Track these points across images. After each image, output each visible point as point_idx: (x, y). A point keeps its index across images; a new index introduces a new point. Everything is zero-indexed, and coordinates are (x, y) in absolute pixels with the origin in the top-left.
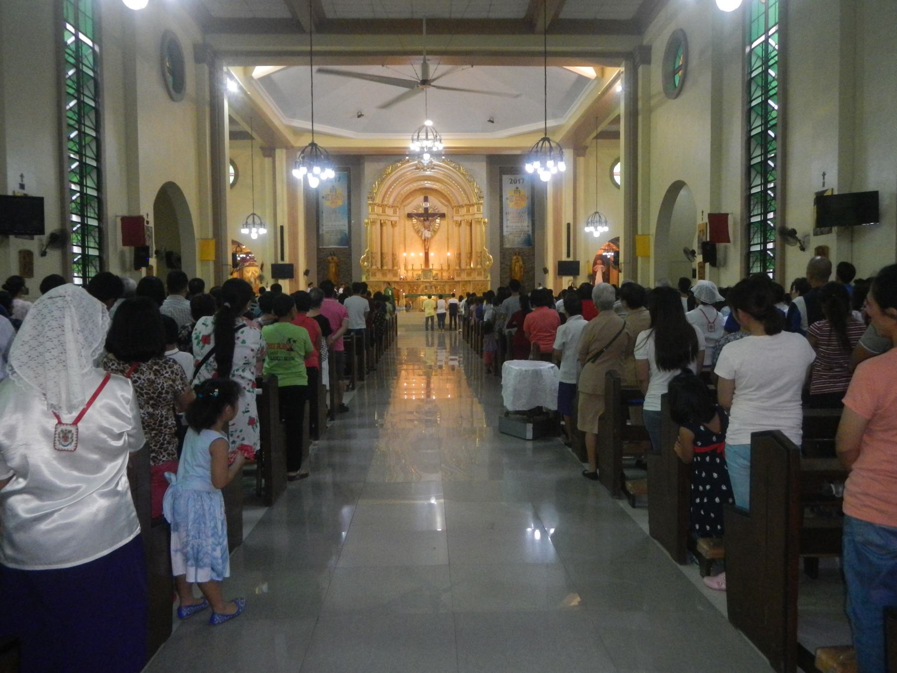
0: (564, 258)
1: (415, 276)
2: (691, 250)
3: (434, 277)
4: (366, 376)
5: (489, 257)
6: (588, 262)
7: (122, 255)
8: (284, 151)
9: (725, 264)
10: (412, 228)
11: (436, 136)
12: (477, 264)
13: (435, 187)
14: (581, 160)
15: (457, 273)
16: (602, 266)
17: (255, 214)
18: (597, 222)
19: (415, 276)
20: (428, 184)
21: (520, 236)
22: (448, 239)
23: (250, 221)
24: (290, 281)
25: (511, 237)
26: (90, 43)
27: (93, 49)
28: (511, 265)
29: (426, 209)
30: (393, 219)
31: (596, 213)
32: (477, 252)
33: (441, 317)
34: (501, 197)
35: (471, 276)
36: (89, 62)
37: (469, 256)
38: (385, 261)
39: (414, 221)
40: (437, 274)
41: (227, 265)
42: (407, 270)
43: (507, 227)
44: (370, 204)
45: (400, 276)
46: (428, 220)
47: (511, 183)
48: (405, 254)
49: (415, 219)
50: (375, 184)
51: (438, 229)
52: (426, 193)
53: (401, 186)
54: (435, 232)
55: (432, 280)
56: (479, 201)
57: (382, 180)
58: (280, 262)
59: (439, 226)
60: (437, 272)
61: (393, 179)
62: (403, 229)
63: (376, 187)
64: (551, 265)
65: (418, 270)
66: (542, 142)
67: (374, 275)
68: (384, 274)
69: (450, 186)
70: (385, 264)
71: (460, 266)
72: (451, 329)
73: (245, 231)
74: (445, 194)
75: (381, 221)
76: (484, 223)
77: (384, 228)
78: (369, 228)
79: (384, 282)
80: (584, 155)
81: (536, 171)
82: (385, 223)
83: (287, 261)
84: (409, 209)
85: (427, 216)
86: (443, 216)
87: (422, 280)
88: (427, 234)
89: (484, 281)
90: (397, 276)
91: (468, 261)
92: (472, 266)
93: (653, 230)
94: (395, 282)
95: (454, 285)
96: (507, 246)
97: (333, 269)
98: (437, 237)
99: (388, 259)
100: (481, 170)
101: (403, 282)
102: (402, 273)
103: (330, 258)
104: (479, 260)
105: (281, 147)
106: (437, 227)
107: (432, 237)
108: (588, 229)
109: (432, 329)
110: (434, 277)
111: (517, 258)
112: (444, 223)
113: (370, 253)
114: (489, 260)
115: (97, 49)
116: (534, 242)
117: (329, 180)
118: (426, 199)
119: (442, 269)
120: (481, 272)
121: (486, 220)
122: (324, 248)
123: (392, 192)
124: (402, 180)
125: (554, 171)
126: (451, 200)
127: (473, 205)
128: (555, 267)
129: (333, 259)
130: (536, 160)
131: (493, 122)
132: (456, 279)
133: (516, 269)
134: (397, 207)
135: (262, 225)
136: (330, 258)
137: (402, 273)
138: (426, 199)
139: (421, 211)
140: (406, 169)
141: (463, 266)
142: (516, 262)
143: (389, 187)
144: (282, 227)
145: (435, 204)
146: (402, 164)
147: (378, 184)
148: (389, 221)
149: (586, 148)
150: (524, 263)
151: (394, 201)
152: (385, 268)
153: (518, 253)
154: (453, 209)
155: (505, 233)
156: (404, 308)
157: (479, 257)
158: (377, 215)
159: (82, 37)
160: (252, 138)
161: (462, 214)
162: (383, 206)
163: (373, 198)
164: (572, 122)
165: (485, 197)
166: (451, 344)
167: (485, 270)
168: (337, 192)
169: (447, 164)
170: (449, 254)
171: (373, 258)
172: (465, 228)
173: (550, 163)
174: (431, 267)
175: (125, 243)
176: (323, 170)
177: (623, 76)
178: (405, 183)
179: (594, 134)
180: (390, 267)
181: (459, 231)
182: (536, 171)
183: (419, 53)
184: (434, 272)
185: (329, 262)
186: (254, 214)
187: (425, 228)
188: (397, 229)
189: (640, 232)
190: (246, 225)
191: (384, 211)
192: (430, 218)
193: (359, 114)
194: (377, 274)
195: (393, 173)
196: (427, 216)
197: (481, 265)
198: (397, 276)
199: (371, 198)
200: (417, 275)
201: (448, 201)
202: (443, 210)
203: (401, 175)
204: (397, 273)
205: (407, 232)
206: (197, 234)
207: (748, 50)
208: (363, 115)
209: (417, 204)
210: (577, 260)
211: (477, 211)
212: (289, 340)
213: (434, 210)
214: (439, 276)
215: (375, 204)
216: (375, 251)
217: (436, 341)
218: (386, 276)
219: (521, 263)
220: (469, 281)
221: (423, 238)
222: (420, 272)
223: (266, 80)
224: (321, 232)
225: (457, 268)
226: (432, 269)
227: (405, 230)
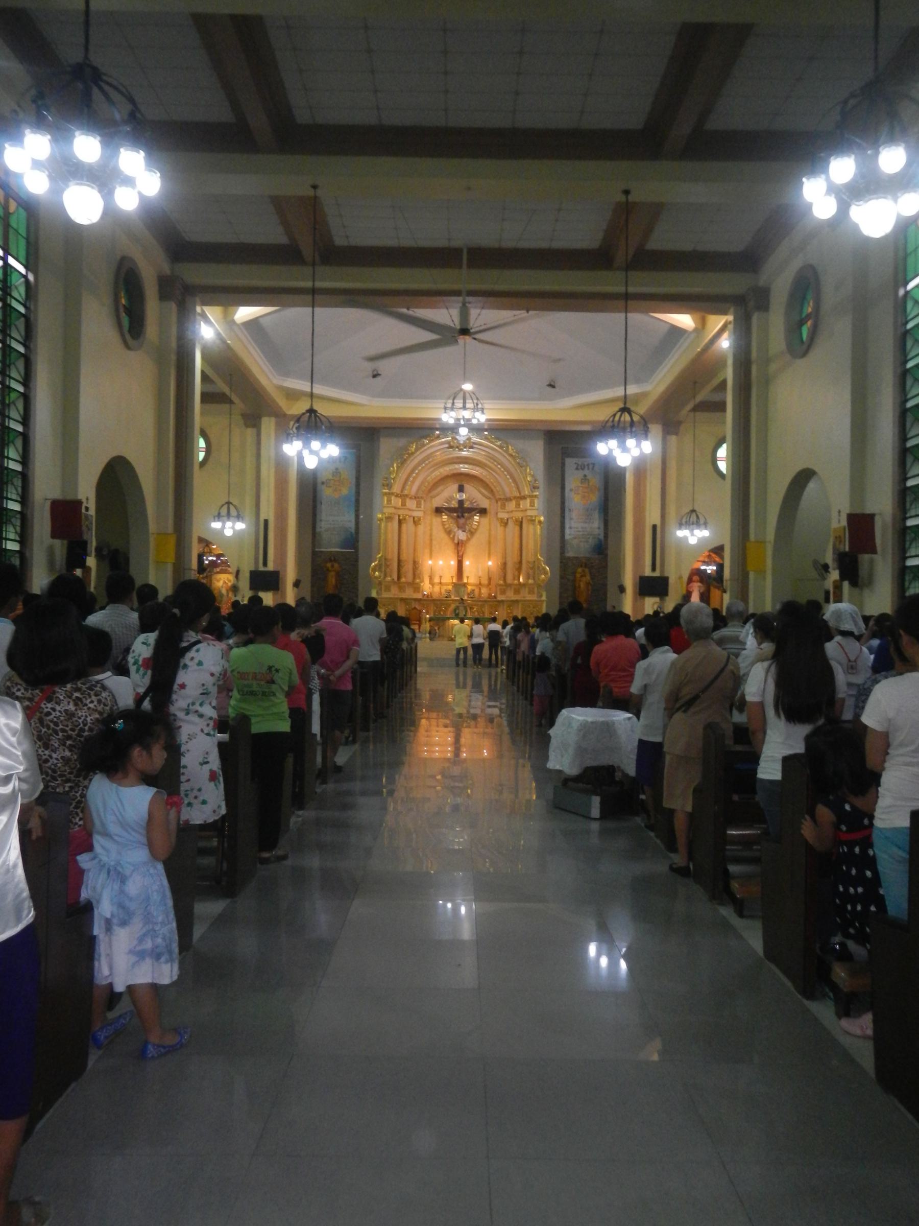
0: (648, 572)
1: (443, 591)
2: (822, 563)
4: (372, 725)
5: (544, 569)
6: (680, 578)
7: (51, 551)
8: (273, 420)
9: (870, 582)
10: (441, 528)
11: (477, 404)
13: (474, 472)
14: (673, 439)
15: (500, 589)
16: (699, 584)
17: (231, 503)
18: (693, 524)
19: (443, 591)
20: (464, 468)
21: (587, 542)
22: (489, 543)
23: (224, 511)
24: (273, 595)
25: (575, 542)
26: (22, 270)
27: (25, 277)
28: (574, 581)
29: (461, 502)
30: (416, 514)
31: (693, 511)
32: (529, 562)
33: (478, 648)
34: (563, 488)
36: (20, 295)
37: (517, 566)
38: (403, 570)
39: (445, 517)
40: (473, 590)
41: (191, 570)
43: (570, 528)
44: (386, 493)
45: (423, 591)
46: (463, 516)
47: (577, 469)
48: (430, 562)
49: (446, 515)
50: (393, 468)
51: (476, 530)
52: (462, 480)
53: (429, 469)
54: (472, 533)
56: (533, 492)
57: (403, 462)
58: (261, 568)
59: (478, 526)
60: (473, 588)
61: (416, 461)
62: (429, 528)
63: (394, 471)
64: (629, 582)
65: (447, 584)
66: (619, 414)
67: (388, 589)
68: (401, 588)
69: (496, 473)
71: (505, 580)
72: (490, 665)
73: (216, 525)
74: (488, 482)
75: (399, 516)
76: (540, 522)
77: (404, 527)
78: (383, 525)
79: (402, 600)
80: (676, 434)
81: (611, 451)
82: (405, 519)
83: (271, 567)
84: (438, 502)
85: (461, 512)
86: (483, 512)
88: (462, 535)
89: (536, 601)
90: (419, 592)
91: (516, 573)
92: (521, 580)
93: (770, 535)
94: (416, 600)
96: (570, 554)
97: (332, 580)
98: (474, 541)
99: (408, 568)
100: (536, 450)
101: (429, 601)
102: (426, 588)
103: (329, 565)
104: (531, 572)
105: (269, 415)
106: (475, 527)
107: (468, 539)
108: (681, 533)
109: (465, 664)
110: (469, 594)
111: (583, 571)
112: (485, 521)
113: (383, 560)
114: (545, 573)
115: (31, 277)
116: (606, 548)
117: (331, 460)
118: (461, 489)
119: (480, 584)
120: (533, 588)
121: (542, 519)
122: (321, 552)
123: (415, 478)
124: (430, 462)
125: (636, 452)
126: (494, 490)
127: (524, 498)
128: (634, 586)
129: (333, 566)
130: (612, 438)
131: (553, 387)
132: (500, 598)
134: (422, 498)
135: (239, 517)
136: (329, 565)
137: (426, 588)
138: (461, 489)
139: (454, 504)
140: (436, 447)
141: (509, 579)
142: (582, 576)
143: (413, 471)
144: (266, 522)
145: (473, 495)
146: (431, 441)
147: (398, 467)
148: (410, 516)
149: (679, 423)
150: (592, 579)
151: (418, 490)
152: (403, 580)
153: (585, 564)
154: (497, 502)
155: (567, 537)
156: (428, 635)
157: (532, 568)
158: (395, 508)
159: (11, 261)
160: (231, 402)
161: (511, 510)
162: (403, 496)
163: (390, 488)
164: (662, 388)
165: (542, 489)
166: (490, 686)
167: (539, 586)
168: (342, 478)
169: (492, 443)
170: (490, 563)
171: (387, 566)
172: (512, 528)
173: (631, 442)
174: (465, 581)
175: (55, 535)
176: (324, 446)
177: (731, 327)
178: (433, 466)
179: (690, 406)
180: (410, 579)
181: (505, 531)
182: (611, 451)
183: (457, 293)
184: (470, 588)
185: (328, 570)
186: (229, 503)
187: (459, 527)
188: (421, 528)
189: (752, 537)
190: (218, 517)
191: (404, 504)
192: (466, 515)
193: (375, 373)
195: (418, 453)
196: (461, 512)
197: (534, 579)
199: (388, 485)
200: (446, 591)
201: (492, 491)
202: (485, 503)
203: (429, 455)
205: (434, 532)
206: (152, 527)
207: (901, 292)
208: (379, 375)
209: (449, 494)
210: (666, 575)
211: (531, 506)
212: (270, 668)
213: (471, 503)
215: (393, 494)
216: (389, 557)
217: (469, 682)
218: (404, 591)
219: (588, 578)
220: (517, 601)
221: (456, 541)
222: (450, 587)
223: (252, 325)
224: (318, 530)
225: (501, 582)
226: (467, 583)
227: (431, 529)
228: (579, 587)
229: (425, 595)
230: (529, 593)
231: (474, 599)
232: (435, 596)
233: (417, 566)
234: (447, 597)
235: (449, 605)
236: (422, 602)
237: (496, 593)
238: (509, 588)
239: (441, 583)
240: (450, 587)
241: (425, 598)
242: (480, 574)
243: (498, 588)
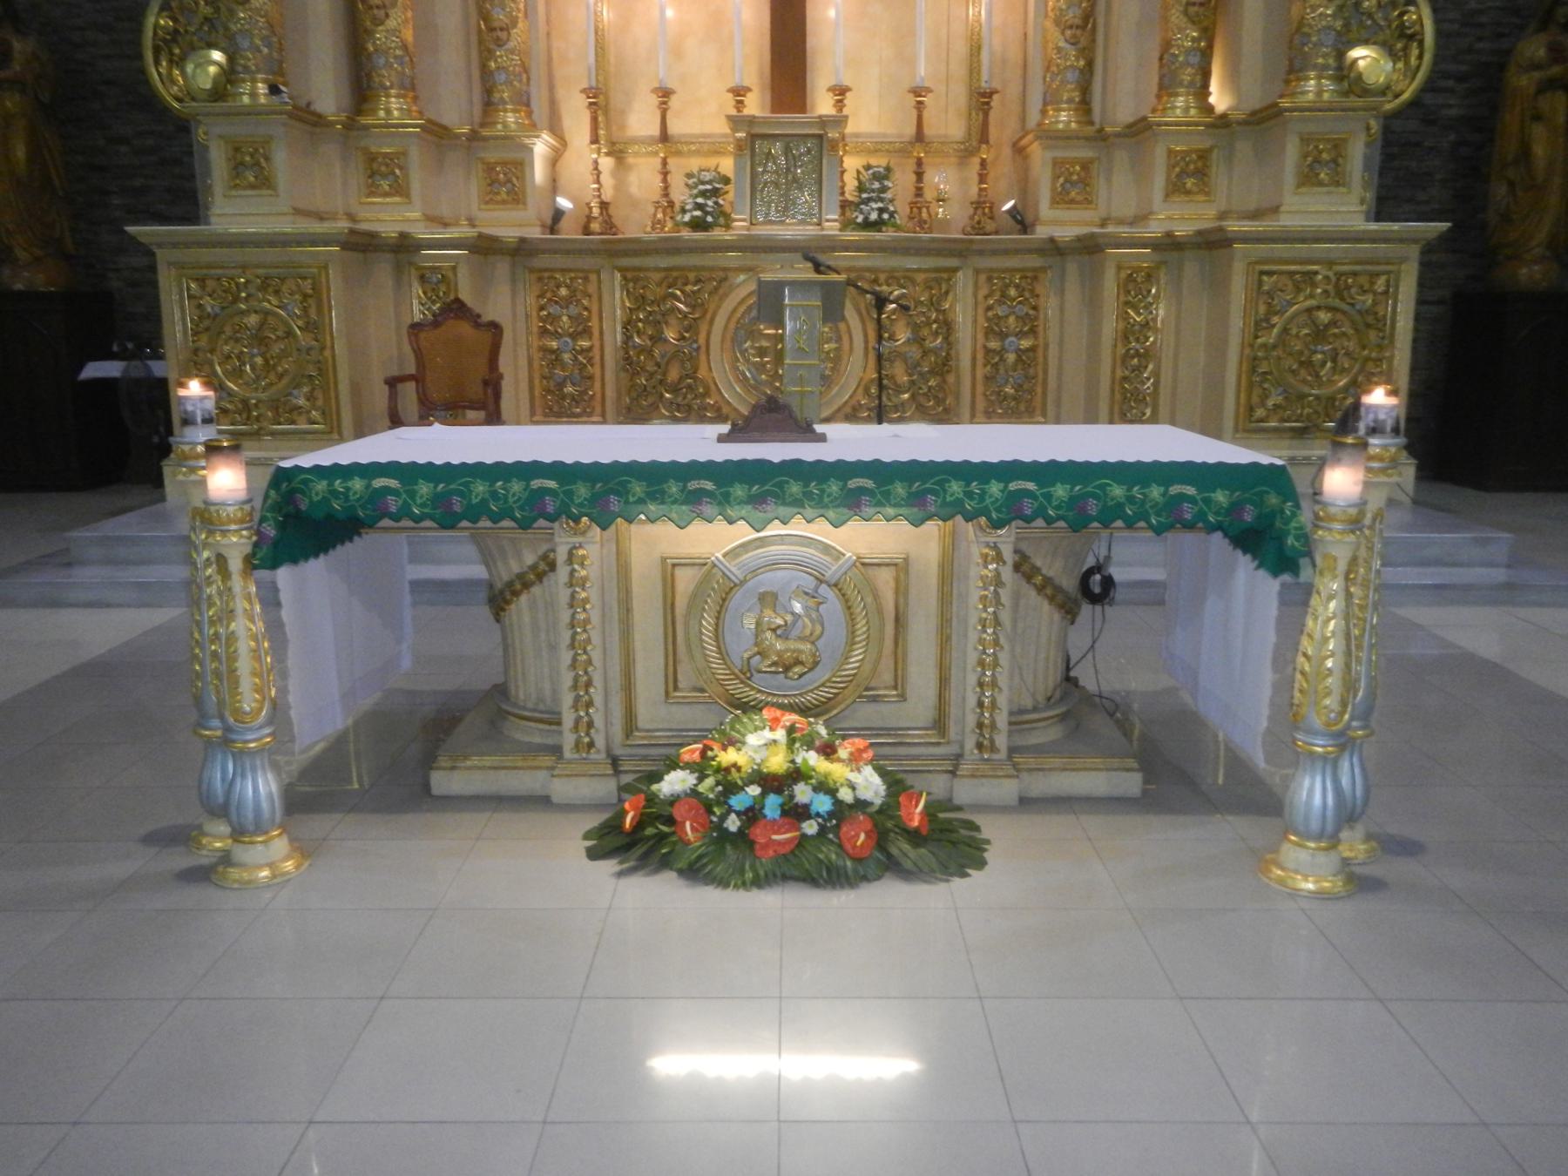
1: (680, 194)
3: (844, 205)
12: (1295, 70)
19: (680, 194)
35: (1205, 188)
40: (883, 176)
42: (618, 152)
55: (832, 227)
60: (879, 162)
70: (387, 76)
87: (740, 225)
92: (1219, 98)
95: (1033, 276)
119: (920, 136)
120: (1338, 146)
133: (1539, 150)
152: (393, 107)
174: (823, 105)
184: (852, 163)
194: (281, 160)
198: (517, 198)
204: (519, 165)
214: (901, 185)
218: (400, 189)
222: (727, 165)
225: (1064, 118)
228: (1525, 153)
229: (558, 214)
230: (1308, 178)
231: (887, 234)
232: (636, 225)
233: (500, 17)
234: (697, 225)
235: (720, 281)
236: (541, 261)
237: (1024, 188)
238: (1121, 157)
239: (664, 137)
240: (727, 165)
241: (569, 231)
242: (922, 72)
243: (1040, 158)
